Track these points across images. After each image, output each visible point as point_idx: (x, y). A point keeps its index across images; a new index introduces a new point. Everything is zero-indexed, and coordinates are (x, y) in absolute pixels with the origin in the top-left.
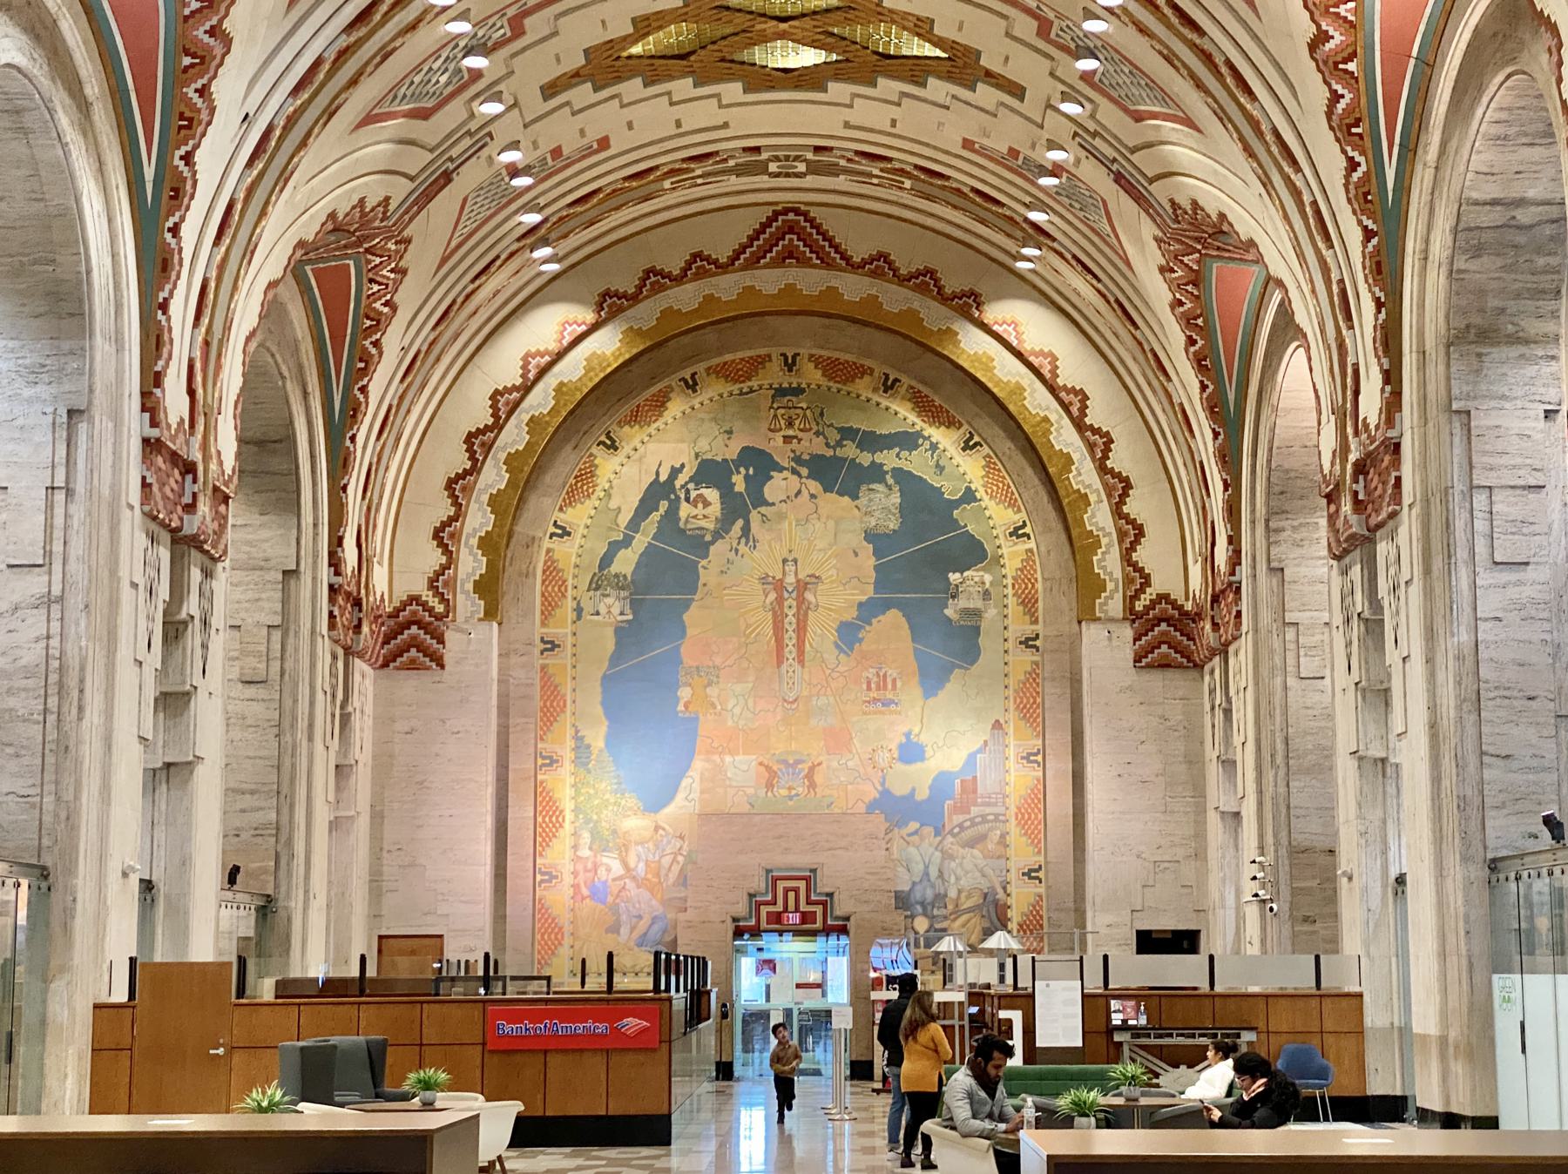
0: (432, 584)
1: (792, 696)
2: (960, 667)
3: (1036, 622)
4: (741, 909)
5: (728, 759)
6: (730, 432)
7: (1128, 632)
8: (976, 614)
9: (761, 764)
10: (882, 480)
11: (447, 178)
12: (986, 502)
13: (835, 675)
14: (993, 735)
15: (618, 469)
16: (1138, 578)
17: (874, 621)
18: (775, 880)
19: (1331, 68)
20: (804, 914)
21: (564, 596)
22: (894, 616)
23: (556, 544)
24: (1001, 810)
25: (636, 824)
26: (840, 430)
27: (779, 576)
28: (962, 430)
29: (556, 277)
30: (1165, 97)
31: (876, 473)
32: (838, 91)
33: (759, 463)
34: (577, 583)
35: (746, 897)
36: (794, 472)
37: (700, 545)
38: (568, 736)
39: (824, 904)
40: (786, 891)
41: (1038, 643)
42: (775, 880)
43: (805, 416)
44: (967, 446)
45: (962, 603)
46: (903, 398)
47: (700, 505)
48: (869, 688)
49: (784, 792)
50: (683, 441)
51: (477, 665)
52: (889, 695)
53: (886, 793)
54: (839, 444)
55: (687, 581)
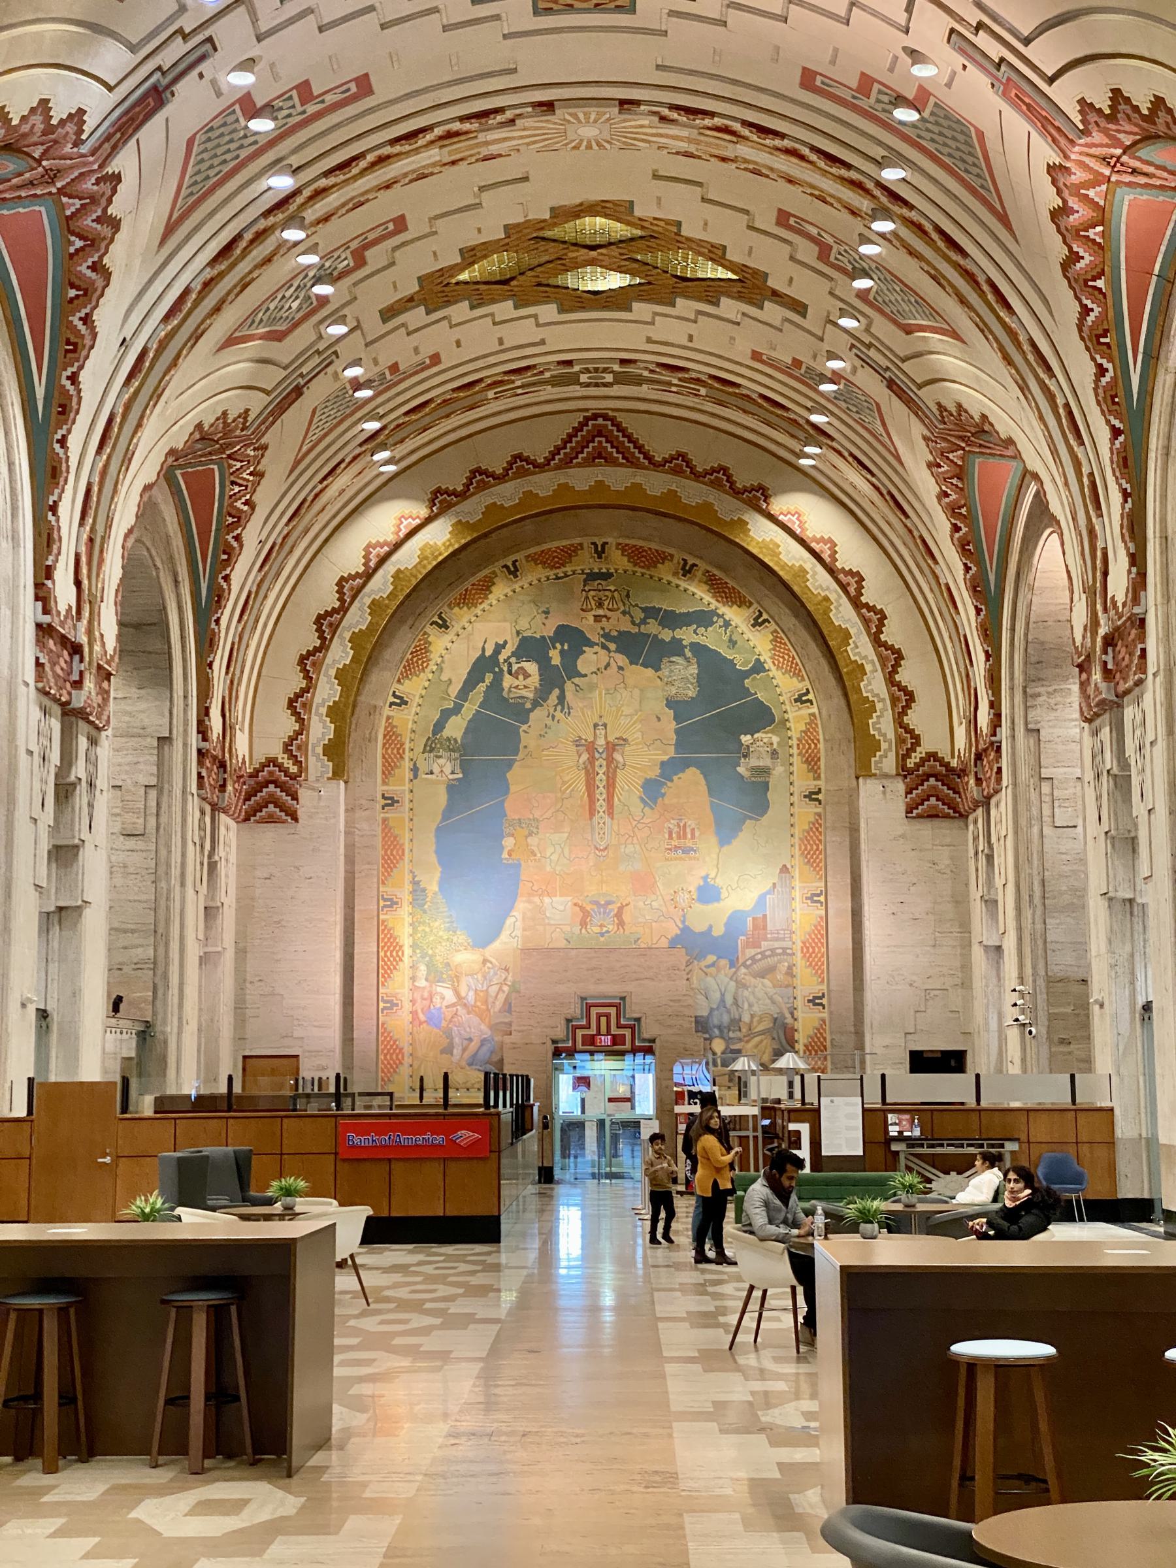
0: (287, 748)
1: (603, 845)
2: (751, 818)
3: (818, 778)
4: (560, 1032)
5: (547, 900)
6: (547, 612)
7: (900, 786)
8: (765, 771)
9: (575, 905)
10: (681, 653)
11: (298, 392)
12: (774, 672)
14: (780, 879)
15: (449, 645)
16: (909, 738)
17: (675, 778)
18: (589, 1006)
19: (1082, 285)
20: (614, 1037)
21: (402, 757)
22: (693, 774)
23: (394, 712)
24: (788, 944)
25: (466, 958)
26: (644, 610)
28: (751, 610)
29: (396, 475)
30: (935, 313)
31: (676, 648)
32: (641, 310)
33: (572, 639)
34: (413, 747)
35: (563, 1022)
36: (604, 647)
37: (521, 713)
38: (407, 882)
39: (632, 1028)
40: (599, 1016)
41: (820, 797)
42: (589, 1007)
43: (613, 597)
44: (757, 623)
45: (753, 762)
46: (700, 581)
47: (521, 677)
48: (671, 837)
49: (597, 930)
50: (505, 620)
51: (326, 819)
52: (689, 843)
53: (686, 930)
54: (644, 621)
55: (509, 744)
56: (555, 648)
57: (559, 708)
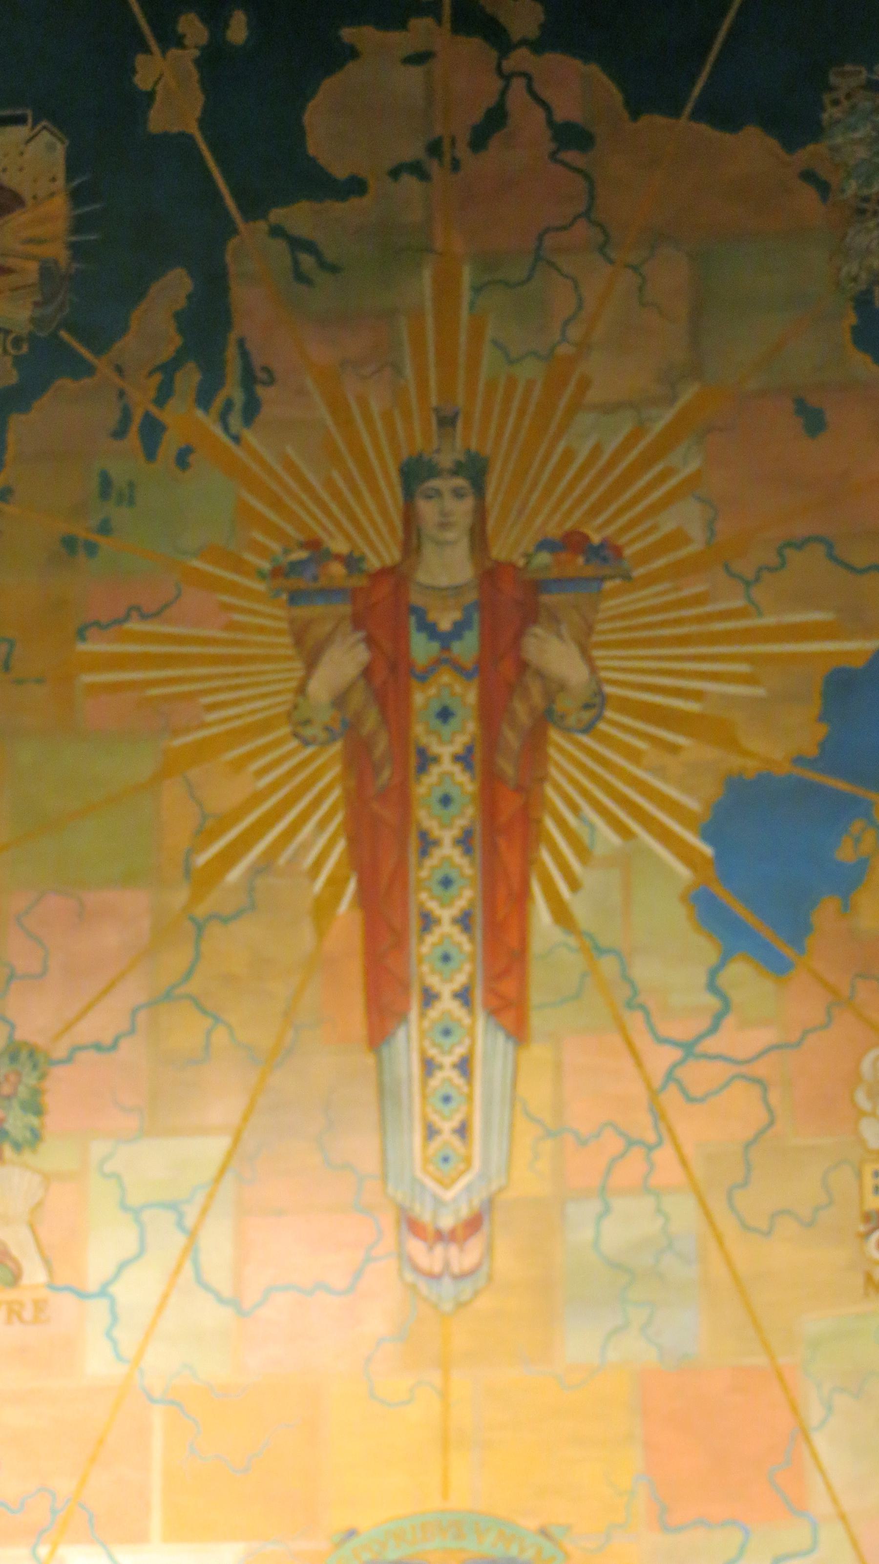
1: (453, 1203)
13: (700, 1075)
27: (383, 553)
56: (170, 39)
57: (190, 378)
